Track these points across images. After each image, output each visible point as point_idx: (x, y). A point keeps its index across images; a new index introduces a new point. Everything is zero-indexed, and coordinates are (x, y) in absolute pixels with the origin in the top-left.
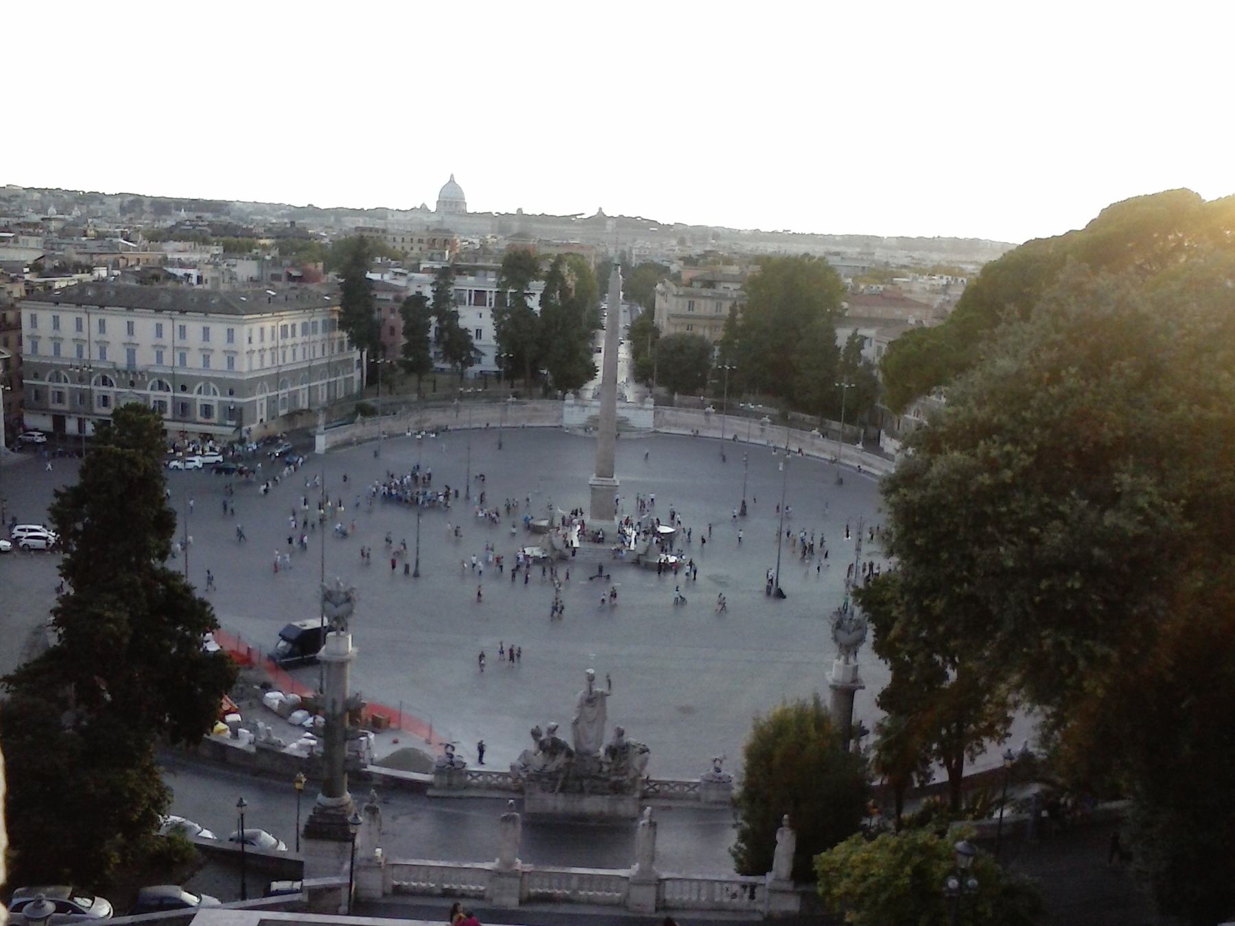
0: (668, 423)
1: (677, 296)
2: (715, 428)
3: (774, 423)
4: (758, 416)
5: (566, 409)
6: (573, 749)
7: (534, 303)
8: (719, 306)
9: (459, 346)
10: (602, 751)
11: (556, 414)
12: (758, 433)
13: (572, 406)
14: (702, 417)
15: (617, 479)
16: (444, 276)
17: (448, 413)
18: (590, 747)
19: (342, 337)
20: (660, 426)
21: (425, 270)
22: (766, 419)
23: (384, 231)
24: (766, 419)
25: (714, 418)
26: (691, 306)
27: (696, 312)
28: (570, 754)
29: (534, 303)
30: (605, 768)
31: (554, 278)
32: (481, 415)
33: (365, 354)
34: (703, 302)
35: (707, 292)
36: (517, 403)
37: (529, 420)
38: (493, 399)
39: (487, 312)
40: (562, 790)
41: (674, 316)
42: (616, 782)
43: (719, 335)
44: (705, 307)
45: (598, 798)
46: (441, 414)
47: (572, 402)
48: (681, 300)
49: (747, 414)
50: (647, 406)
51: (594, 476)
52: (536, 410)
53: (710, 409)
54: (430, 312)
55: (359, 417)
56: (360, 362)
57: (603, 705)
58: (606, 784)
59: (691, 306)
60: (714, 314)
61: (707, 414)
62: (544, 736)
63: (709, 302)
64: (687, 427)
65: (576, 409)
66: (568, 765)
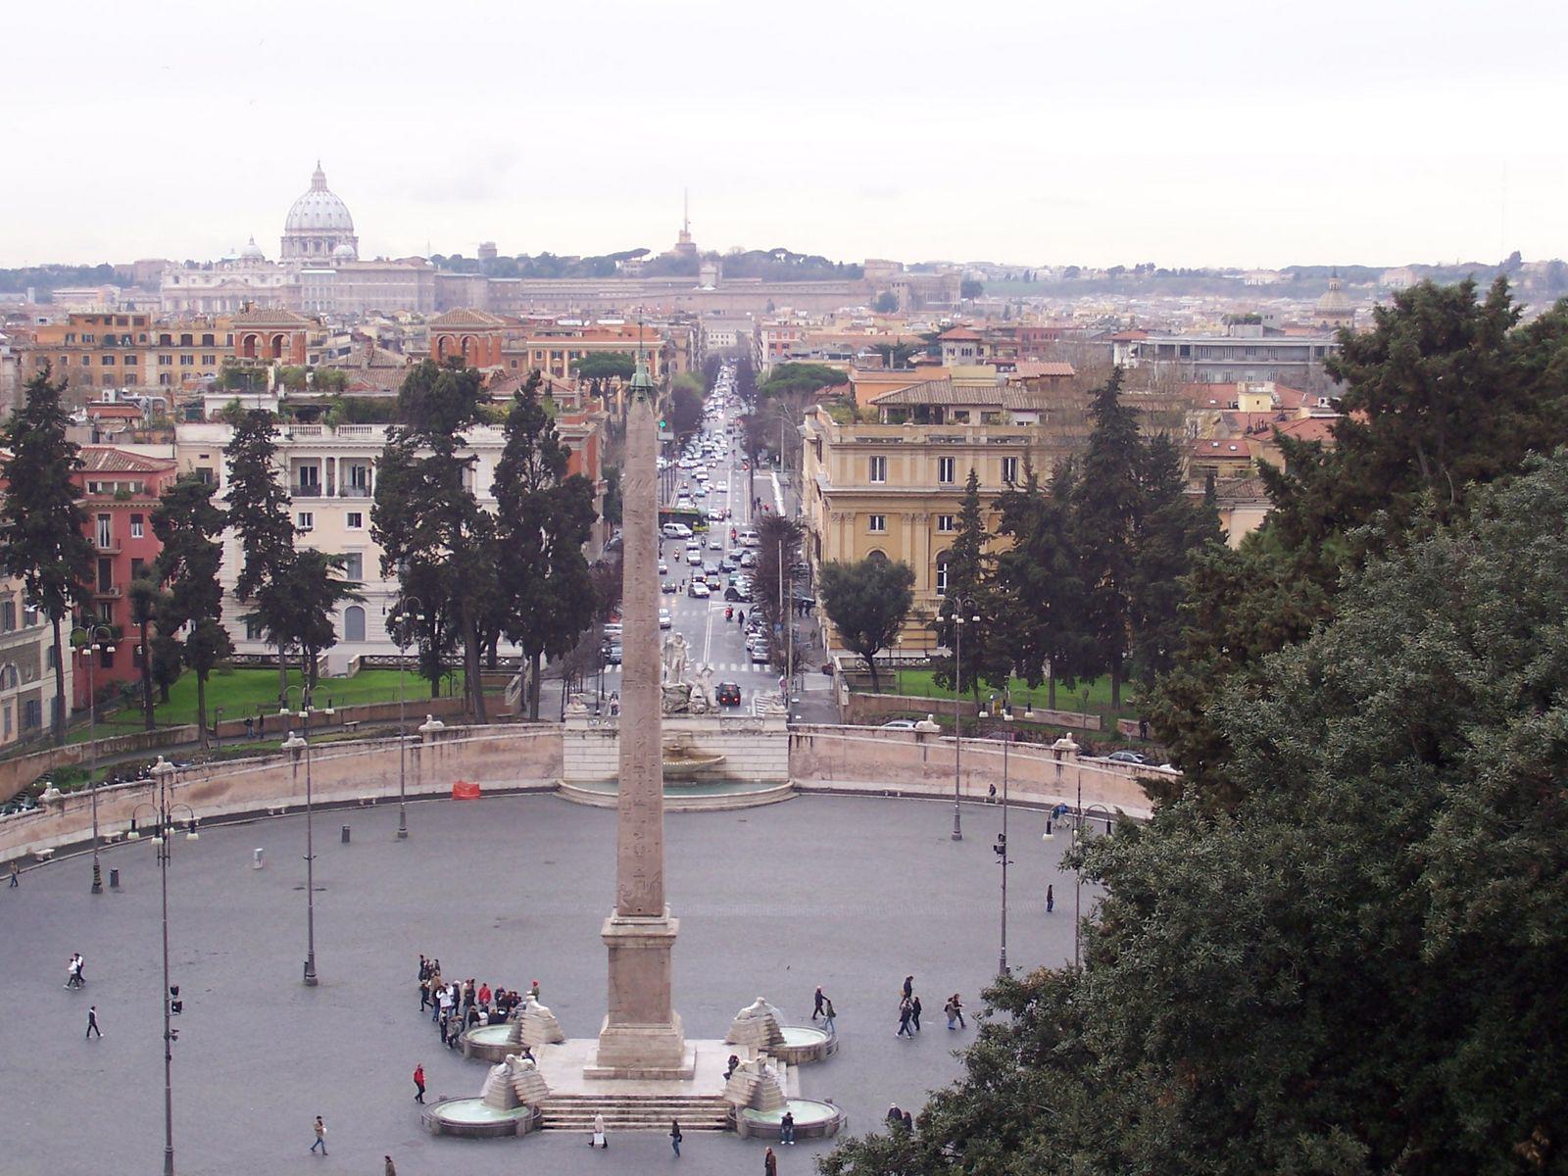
0: (829, 768)
1: (841, 448)
2: (945, 774)
3: (1087, 751)
4: (1045, 734)
5: (569, 742)
7: (481, 482)
8: (946, 470)
9: (299, 597)
12: (1051, 776)
13: (583, 734)
14: (909, 742)
15: (672, 922)
16: (253, 427)
19: (12, 594)
20: (806, 773)
21: (222, 417)
22: (1067, 742)
23: (140, 321)
24: (1067, 742)
25: (939, 745)
26: (877, 468)
27: (890, 484)
29: (481, 482)
31: (527, 420)
32: (354, 770)
33: (66, 626)
34: (906, 459)
35: (914, 432)
36: (443, 734)
37: (477, 776)
38: (389, 723)
39: (365, 507)
41: (835, 497)
43: (947, 539)
44: (914, 473)
47: (583, 725)
48: (850, 458)
49: (1022, 733)
51: (614, 917)
52: (490, 748)
54: (218, 523)
55: (50, 793)
56: (55, 651)
59: (877, 468)
60: (934, 485)
61: (920, 736)
63: (921, 459)
65: (595, 741)
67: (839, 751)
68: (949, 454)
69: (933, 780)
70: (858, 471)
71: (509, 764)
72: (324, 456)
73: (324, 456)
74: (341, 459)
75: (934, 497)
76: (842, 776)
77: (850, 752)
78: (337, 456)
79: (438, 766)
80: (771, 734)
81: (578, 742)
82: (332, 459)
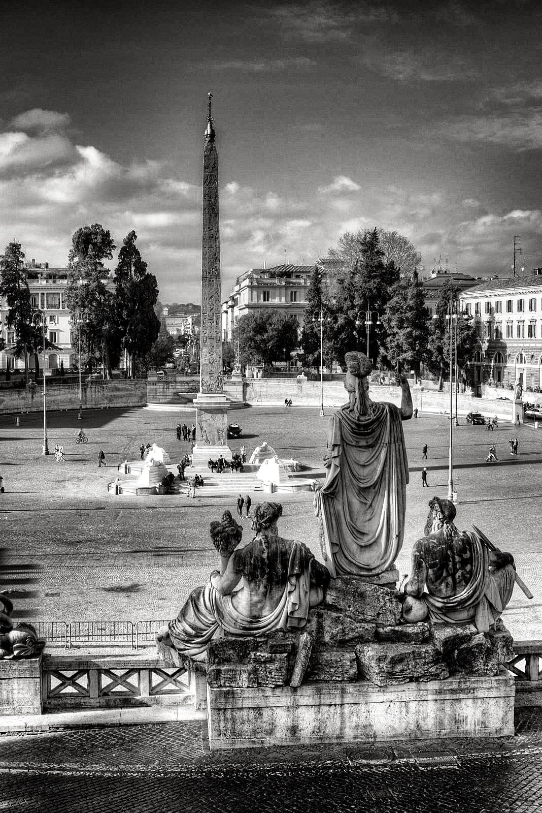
5: (148, 387)
6: (330, 566)
10: (405, 566)
11: (138, 393)
13: (154, 383)
17: (23, 394)
18: (368, 558)
28: (320, 579)
30: (417, 609)
40: (307, 679)
42: (452, 643)
45: (409, 691)
46: (15, 396)
50: (234, 379)
53: (302, 377)
57: (398, 439)
58: (429, 648)
62: (250, 537)
63: (283, 291)
64: (278, 397)
65: (160, 386)
66: (319, 609)
67: (264, 389)
68: (294, 290)
69: (304, 399)
70: (258, 298)
71: (124, 396)
72: (40, 292)
73: (40, 292)
74: (47, 294)
75: (289, 307)
76: (265, 400)
77: (269, 389)
78: (45, 292)
79: (94, 396)
80: (234, 383)
81: (154, 387)
82: (43, 294)
